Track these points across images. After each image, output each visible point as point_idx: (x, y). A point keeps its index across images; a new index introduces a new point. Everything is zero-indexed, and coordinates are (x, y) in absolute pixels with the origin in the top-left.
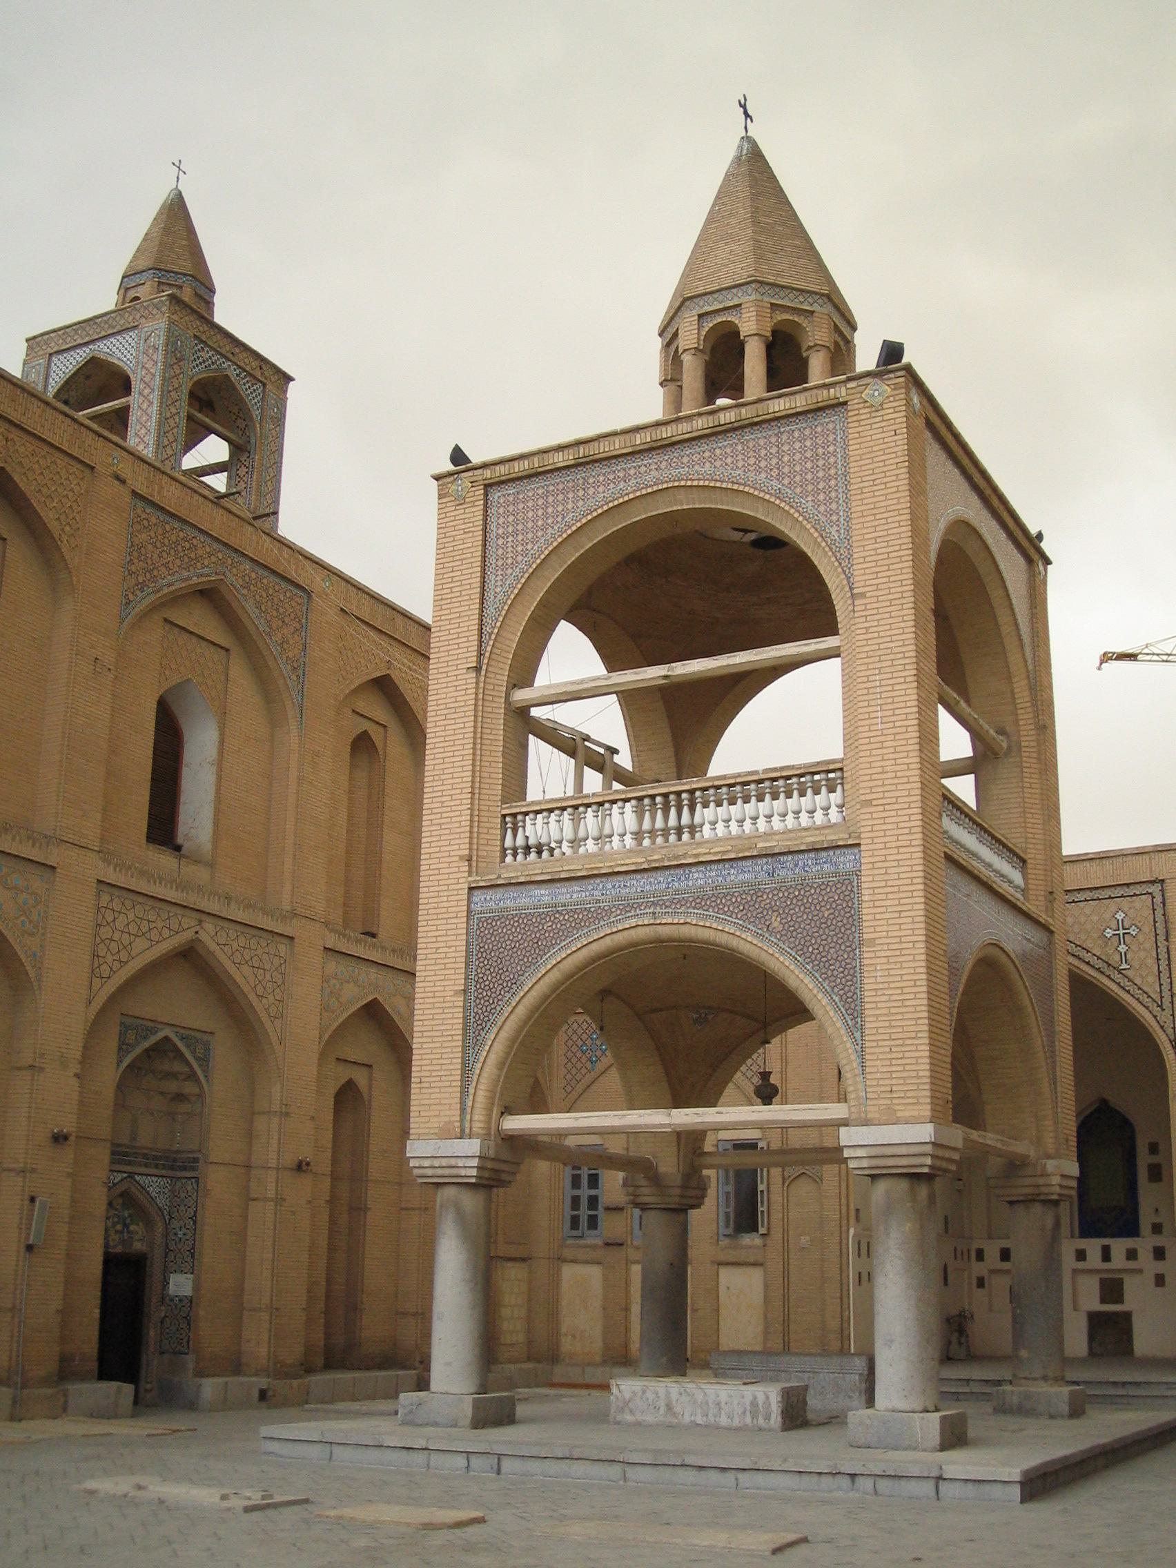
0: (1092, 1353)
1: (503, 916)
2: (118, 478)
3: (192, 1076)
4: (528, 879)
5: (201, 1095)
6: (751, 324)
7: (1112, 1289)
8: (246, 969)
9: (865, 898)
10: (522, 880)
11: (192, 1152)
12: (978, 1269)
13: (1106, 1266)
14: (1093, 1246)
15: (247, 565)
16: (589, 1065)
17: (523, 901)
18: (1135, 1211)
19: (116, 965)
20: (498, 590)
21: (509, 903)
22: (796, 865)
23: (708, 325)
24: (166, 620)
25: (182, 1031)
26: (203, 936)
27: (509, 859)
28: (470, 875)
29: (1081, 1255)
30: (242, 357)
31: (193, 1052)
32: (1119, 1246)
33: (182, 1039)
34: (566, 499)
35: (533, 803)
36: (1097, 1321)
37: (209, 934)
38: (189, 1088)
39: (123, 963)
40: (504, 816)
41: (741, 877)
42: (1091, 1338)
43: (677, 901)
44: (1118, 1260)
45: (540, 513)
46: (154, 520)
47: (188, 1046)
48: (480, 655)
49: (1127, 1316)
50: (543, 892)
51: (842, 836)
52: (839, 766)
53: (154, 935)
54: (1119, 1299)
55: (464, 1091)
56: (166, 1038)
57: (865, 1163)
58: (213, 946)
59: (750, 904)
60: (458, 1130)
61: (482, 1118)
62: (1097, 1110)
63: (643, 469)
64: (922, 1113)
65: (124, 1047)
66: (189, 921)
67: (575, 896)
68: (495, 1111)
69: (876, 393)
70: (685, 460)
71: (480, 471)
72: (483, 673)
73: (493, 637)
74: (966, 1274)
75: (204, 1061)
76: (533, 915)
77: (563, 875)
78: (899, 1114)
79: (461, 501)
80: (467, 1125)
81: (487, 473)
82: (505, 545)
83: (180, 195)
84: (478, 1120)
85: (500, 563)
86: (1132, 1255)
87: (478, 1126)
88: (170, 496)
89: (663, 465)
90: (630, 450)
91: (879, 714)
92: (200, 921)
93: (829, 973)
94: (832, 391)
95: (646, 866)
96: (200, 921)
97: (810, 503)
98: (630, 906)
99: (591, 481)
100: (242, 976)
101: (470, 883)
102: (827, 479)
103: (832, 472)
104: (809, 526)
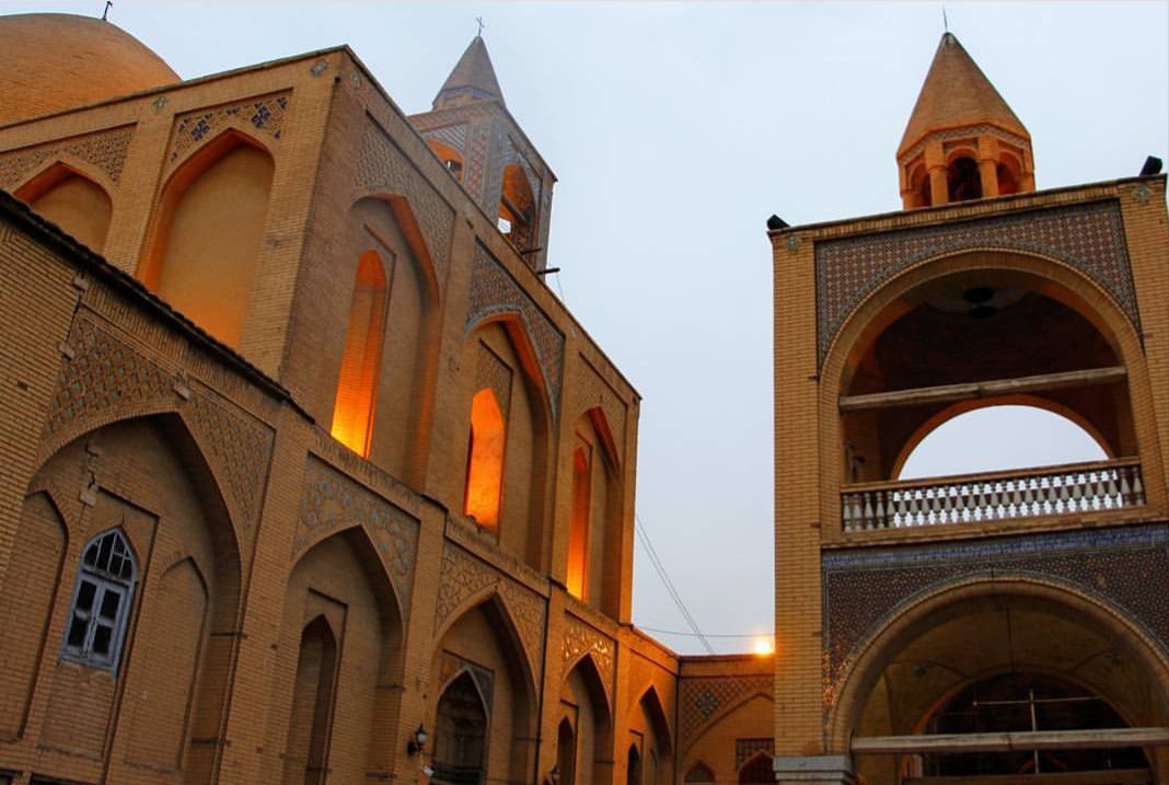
1: (854, 573)
2: (469, 223)
3: (479, 708)
4: (876, 543)
5: (483, 723)
6: (986, 152)
8: (521, 620)
10: (871, 544)
11: (474, 768)
15: (533, 308)
16: (704, 717)
19: (451, 608)
21: (857, 562)
22: (1114, 537)
23: (951, 151)
24: (482, 342)
25: (478, 669)
26: (500, 593)
27: (848, 529)
28: (821, 539)
30: (531, 156)
31: (481, 686)
33: (476, 673)
34: (885, 258)
35: (903, 482)
37: (504, 590)
38: (472, 716)
39: (455, 606)
40: (842, 495)
41: (1066, 546)
43: (1008, 565)
45: (864, 264)
46: (485, 261)
47: (479, 680)
48: (819, 368)
50: (888, 554)
51: (1155, 514)
52: (1137, 462)
53: (472, 586)
56: (466, 673)
58: (505, 601)
59: (1079, 568)
60: (822, 749)
61: (841, 739)
65: (443, 677)
66: (491, 577)
67: (919, 558)
68: (849, 734)
70: (986, 232)
72: (822, 382)
73: (829, 354)
75: (489, 694)
76: (881, 573)
77: (909, 541)
79: (794, 251)
80: (829, 744)
81: (817, 233)
83: (481, 41)
84: (838, 739)
85: (830, 300)
87: (838, 746)
88: (497, 246)
89: (968, 235)
92: (499, 580)
93: (1153, 622)
95: (983, 535)
96: (499, 580)
98: (969, 567)
100: (520, 626)
101: (822, 545)
102: (1107, 251)
103: (1111, 247)
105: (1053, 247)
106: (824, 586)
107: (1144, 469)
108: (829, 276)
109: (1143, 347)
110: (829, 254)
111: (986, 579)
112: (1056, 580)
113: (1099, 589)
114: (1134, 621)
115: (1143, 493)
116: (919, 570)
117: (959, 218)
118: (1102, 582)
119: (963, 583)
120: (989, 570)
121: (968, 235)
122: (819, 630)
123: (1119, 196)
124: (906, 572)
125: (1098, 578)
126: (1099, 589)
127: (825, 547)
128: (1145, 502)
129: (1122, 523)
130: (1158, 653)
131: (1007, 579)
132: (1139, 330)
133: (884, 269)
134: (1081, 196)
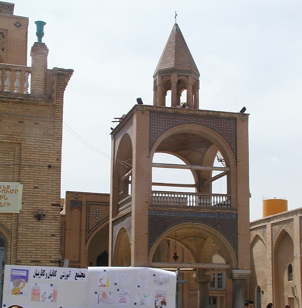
4: (164, 210)
9: (238, 225)
17: (161, 214)
20: (153, 138)
40: (152, 193)
52: (230, 196)
55: (148, 257)
57: (237, 277)
63: (189, 119)
64: (249, 268)
69: (243, 118)
71: (149, 107)
78: (244, 268)
81: (151, 108)
82: (154, 128)
90: (187, 114)
91: (242, 188)
94: (234, 115)
95: (192, 211)
97: (227, 138)
99: (177, 118)
101: (149, 208)
104: (227, 143)
105: (217, 129)
106: (149, 220)
107: (231, 198)
108: (153, 124)
109: (236, 164)
110: (153, 116)
111: (191, 223)
112: (208, 225)
113: (218, 229)
114: (226, 238)
115: (230, 205)
116: (174, 218)
117: (193, 114)
118: (219, 227)
119: (185, 223)
120: (192, 220)
121: (194, 120)
122: (147, 233)
123: (237, 117)
124: (171, 219)
125: (219, 226)
126: (218, 229)
127: (150, 209)
128: (230, 207)
129: (226, 212)
130: (231, 247)
131: (196, 223)
132: (236, 159)
133: (170, 125)
134: (227, 115)
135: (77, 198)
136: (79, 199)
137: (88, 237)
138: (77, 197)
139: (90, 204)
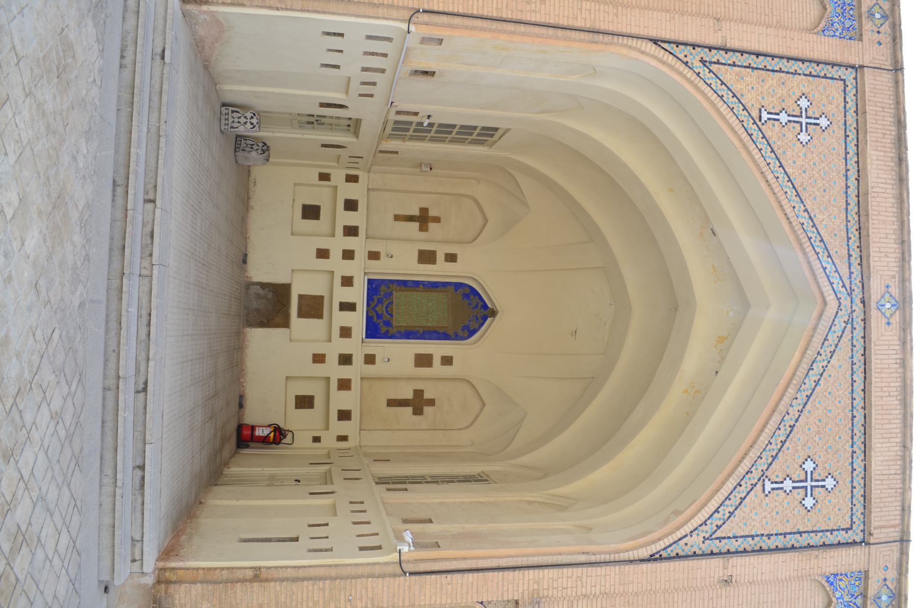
0: (249, 284)
7: (313, 307)
12: (338, 177)
13: (336, 306)
14: (358, 294)
18: (387, 336)
29: (347, 281)
32: (357, 320)
36: (281, 292)
42: (263, 285)
44: (342, 319)
49: (286, 324)
54: (301, 315)
62: (485, 306)
74: (335, 164)
86: (346, 332)
135: (871, 15)
136: (867, 26)
137: (681, 56)
138: (878, 16)
139: (846, 86)
